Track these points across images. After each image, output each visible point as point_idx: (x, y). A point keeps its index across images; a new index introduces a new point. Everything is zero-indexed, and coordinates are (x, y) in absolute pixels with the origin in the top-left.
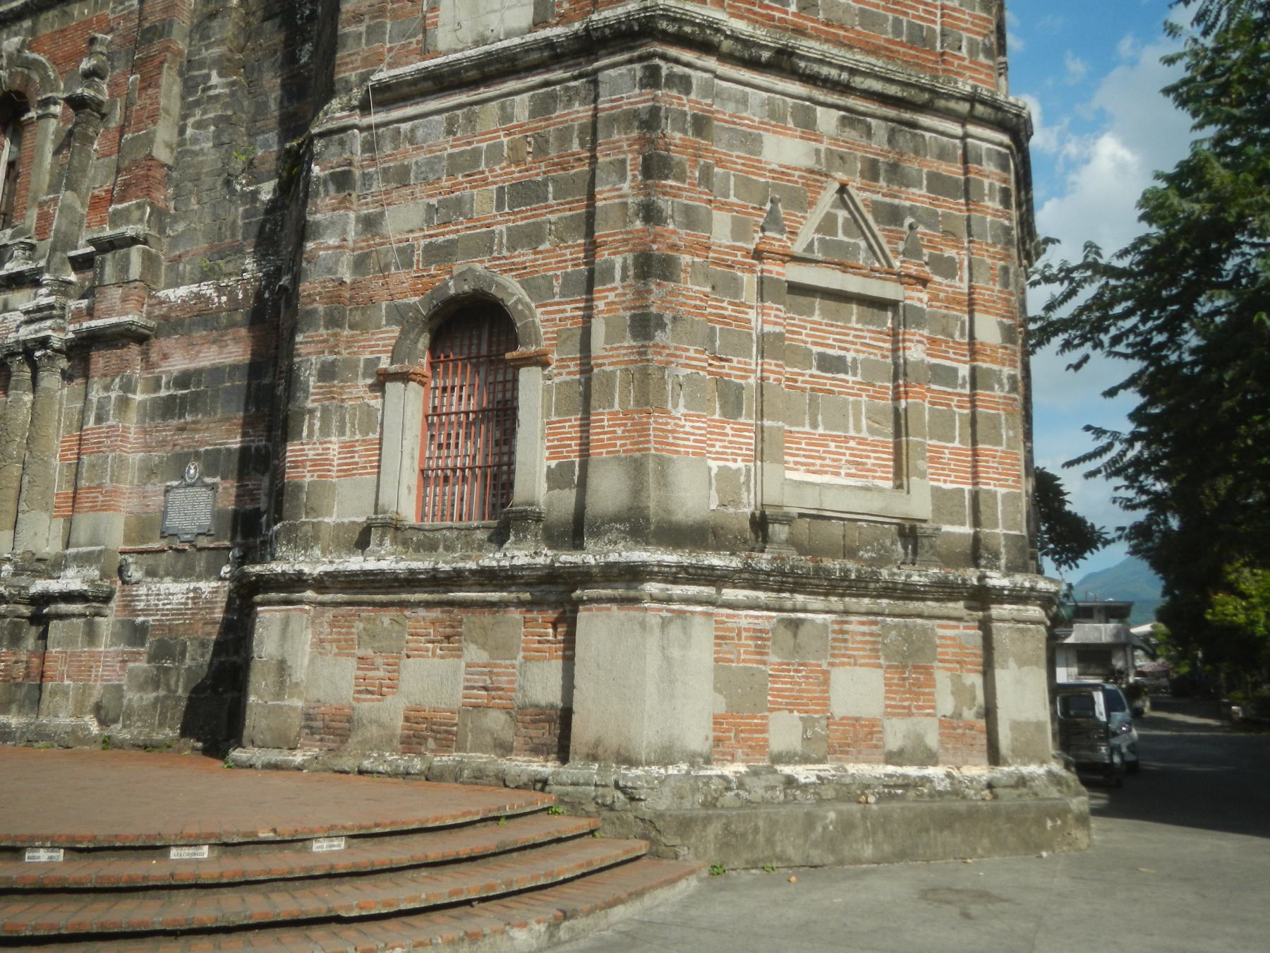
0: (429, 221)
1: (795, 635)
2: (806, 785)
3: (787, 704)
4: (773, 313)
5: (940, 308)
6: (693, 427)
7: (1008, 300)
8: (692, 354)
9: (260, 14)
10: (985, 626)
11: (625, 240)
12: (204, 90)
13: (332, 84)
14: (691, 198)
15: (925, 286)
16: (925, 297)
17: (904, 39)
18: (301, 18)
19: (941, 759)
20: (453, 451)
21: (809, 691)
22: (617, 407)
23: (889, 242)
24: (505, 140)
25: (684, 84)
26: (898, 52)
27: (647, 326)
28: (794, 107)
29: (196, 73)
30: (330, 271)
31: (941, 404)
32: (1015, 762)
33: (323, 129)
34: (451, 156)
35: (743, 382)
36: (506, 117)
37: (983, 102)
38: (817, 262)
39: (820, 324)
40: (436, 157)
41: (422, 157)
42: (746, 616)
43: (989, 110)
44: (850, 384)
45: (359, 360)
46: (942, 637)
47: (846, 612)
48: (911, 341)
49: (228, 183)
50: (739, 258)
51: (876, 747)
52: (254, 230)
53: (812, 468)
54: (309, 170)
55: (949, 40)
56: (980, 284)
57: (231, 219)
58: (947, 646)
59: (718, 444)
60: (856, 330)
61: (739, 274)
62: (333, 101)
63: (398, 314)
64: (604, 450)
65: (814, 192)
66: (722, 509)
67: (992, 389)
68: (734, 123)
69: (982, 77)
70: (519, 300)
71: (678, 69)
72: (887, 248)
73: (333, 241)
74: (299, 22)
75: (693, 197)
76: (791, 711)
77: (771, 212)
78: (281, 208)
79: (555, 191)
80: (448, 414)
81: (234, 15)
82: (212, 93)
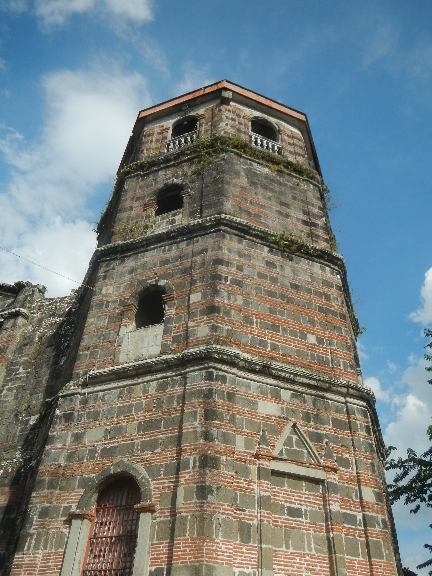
0: (105, 437)
4: (265, 485)
5: (344, 483)
6: (226, 548)
7: (376, 480)
8: (226, 507)
9: (46, 345)
11: (195, 448)
12: (15, 375)
13: (72, 374)
14: (226, 429)
15: (336, 472)
16: (337, 478)
17: (316, 362)
18: (63, 347)
20: (101, 560)
22: (188, 536)
23: (317, 451)
24: (144, 401)
25: (224, 379)
26: (314, 367)
27: (204, 492)
28: (271, 389)
29: (13, 368)
30: (55, 460)
31: (350, 535)
33: (64, 394)
34: (119, 407)
35: (251, 522)
36: (145, 391)
37: (352, 388)
38: (285, 460)
40: (112, 407)
41: (106, 407)
43: (356, 391)
44: (304, 524)
45: (61, 507)
48: (332, 501)
49: (16, 416)
52: (24, 438)
54: (54, 412)
55: (335, 362)
56: (362, 471)
57: (14, 432)
59: (239, 558)
60: (305, 494)
61: (248, 465)
62: (71, 382)
63: (84, 483)
64: (180, 561)
65: (282, 427)
67: (375, 527)
68: (245, 396)
69: (351, 377)
70: (143, 477)
71: (221, 373)
72: (316, 453)
73: (59, 446)
74: (62, 348)
75: (227, 429)
77: (262, 436)
78: (38, 428)
79: (164, 425)
80: (101, 538)
81: (35, 344)
82: (18, 376)
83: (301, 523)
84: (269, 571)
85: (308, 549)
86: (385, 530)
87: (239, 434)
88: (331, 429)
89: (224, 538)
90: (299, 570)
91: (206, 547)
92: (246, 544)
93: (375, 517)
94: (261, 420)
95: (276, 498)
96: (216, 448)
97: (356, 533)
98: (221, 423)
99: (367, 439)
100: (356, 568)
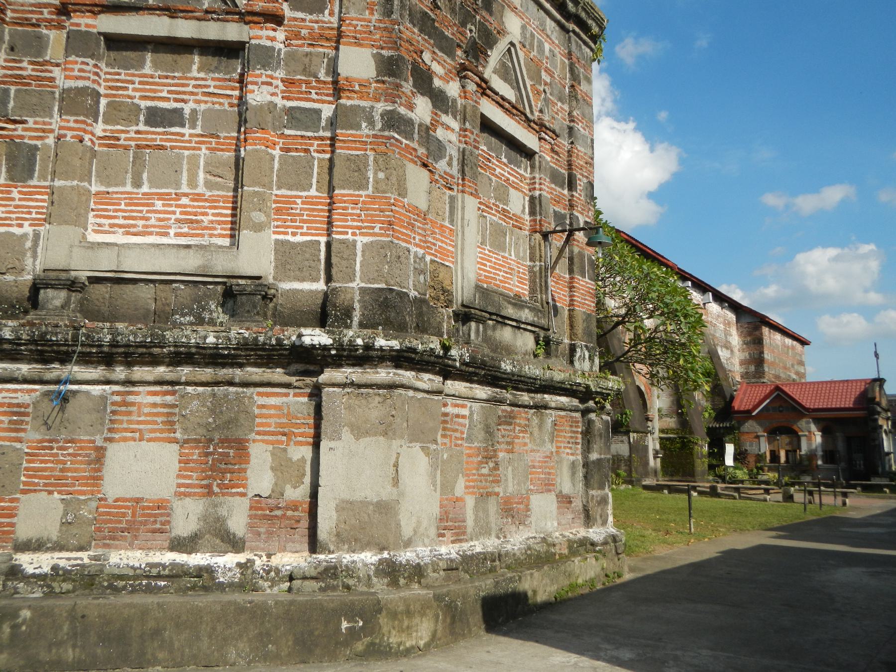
1: (62, 409)
2: (34, 576)
3: (45, 485)
5: (302, 46)
10: (316, 393)
19: (247, 544)
21: (76, 470)
31: (297, 150)
32: (338, 549)
39: (152, 77)
44: (187, 138)
46: (263, 406)
47: (133, 383)
48: (256, 83)
50: (46, 13)
53: (132, 230)
56: (353, 14)
58: (270, 416)
60: (196, 79)
61: (45, 31)
67: (359, 127)
76: (50, 493)
83: (178, 138)
84: (64, 228)
85: (188, 185)
86: (386, 133)
90: (162, 223)
92: (19, 184)
95: (120, 92)
97: (312, 145)
100: (298, 211)
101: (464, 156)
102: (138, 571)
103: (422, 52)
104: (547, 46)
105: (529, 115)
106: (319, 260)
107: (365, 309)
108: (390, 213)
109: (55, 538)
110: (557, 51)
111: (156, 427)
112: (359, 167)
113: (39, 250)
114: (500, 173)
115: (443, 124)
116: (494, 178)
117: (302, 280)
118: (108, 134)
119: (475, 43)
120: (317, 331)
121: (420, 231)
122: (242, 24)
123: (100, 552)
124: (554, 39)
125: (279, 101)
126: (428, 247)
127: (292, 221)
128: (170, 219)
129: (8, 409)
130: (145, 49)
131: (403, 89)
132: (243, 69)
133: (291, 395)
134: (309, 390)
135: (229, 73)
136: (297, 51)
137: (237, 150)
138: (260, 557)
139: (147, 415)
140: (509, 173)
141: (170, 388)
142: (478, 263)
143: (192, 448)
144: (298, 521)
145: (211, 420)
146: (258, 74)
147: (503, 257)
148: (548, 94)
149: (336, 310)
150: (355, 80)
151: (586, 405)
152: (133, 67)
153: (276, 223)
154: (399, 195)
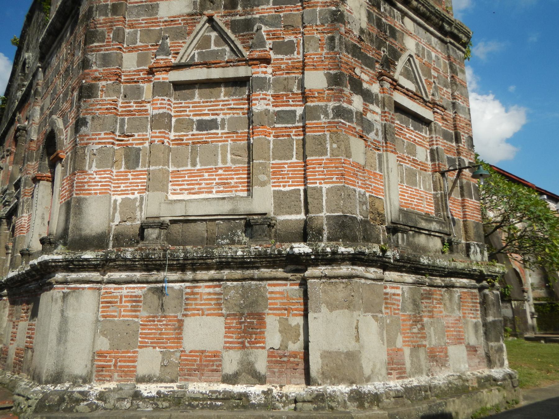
2: (147, 397)
3: (152, 343)
4: (159, 102)
5: (283, 74)
8: (103, 136)
10: (304, 283)
14: (107, 50)
19: (267, 379)
21: (167, 334)
23: (243, 43)
31: (283, 136)
32: (324, 383)
35: (141, 146)
42: (126, 288)
44: (220, 135)
46: (272, 293)
47: (197, 281)
48: (257, 99)
50: (142, 75)
51: (217, 371)
53: (192, 191)
56: (311, 52)
60: (223, 101)
61: (141, 85)
66: (123, 223)
76: (154, 347)
83: (215, 136)
84: (156, 193)
85: (222, 162)
86: (336, 120)
87: (132, 51)
88: (270, 9)
89: (99, 168)
90: (208, 186)
91: (77, 181)
93: (322, 106)
94: (162, 26)
95: (182, 113)
96: (93, 74)
97: (292, 132)
98: (101, 44)
99: (328, 6)
100: (286, 172)
101: (385, 128)
102: (205, 396)
103: (354, 68)
104: (433, 54)
105: (425, 98)
106: (300, 201)
107: (330, 229)
108: (342, 169)
109: (158, 375)
110: (440, 56)
111: (211, 307)
112: (321, 141)
113: (143, 207)
114: (409, 137)
115: (370, 111)
116: (405, 140)
117: (291, 213)
118: (177, 138)
119: (387, 58)
120: (302, 244)
121: (361, 178)
122: (247, 66)
123: (183, 383)
124: (437, 48)
125: (271, 109)
126: (367, 188)
127: (282, 178)
128: (213, 183)
129: (130, 299)
130: (195, 88)
131: (345, 92)
132: (249, 92)
133: (288, 285)
134: (299, 282)
135: (241, 95)
136: (279, 78)
137: (249, 140)
138: (276, 387)
139: (205, 300)
140: (415, 136)
141: (218, 283)
142: (400, 194)
143: (232, 319)
144: (298, 365)
145: (242, 302)
146: (258, 94)
147: (416, 190)
148: (437, 84)
149: (312, 231)
150: (315, 90)
151: (481, 284)
152: (189, 99)
153: (273, 181)
154: (347, 157)
